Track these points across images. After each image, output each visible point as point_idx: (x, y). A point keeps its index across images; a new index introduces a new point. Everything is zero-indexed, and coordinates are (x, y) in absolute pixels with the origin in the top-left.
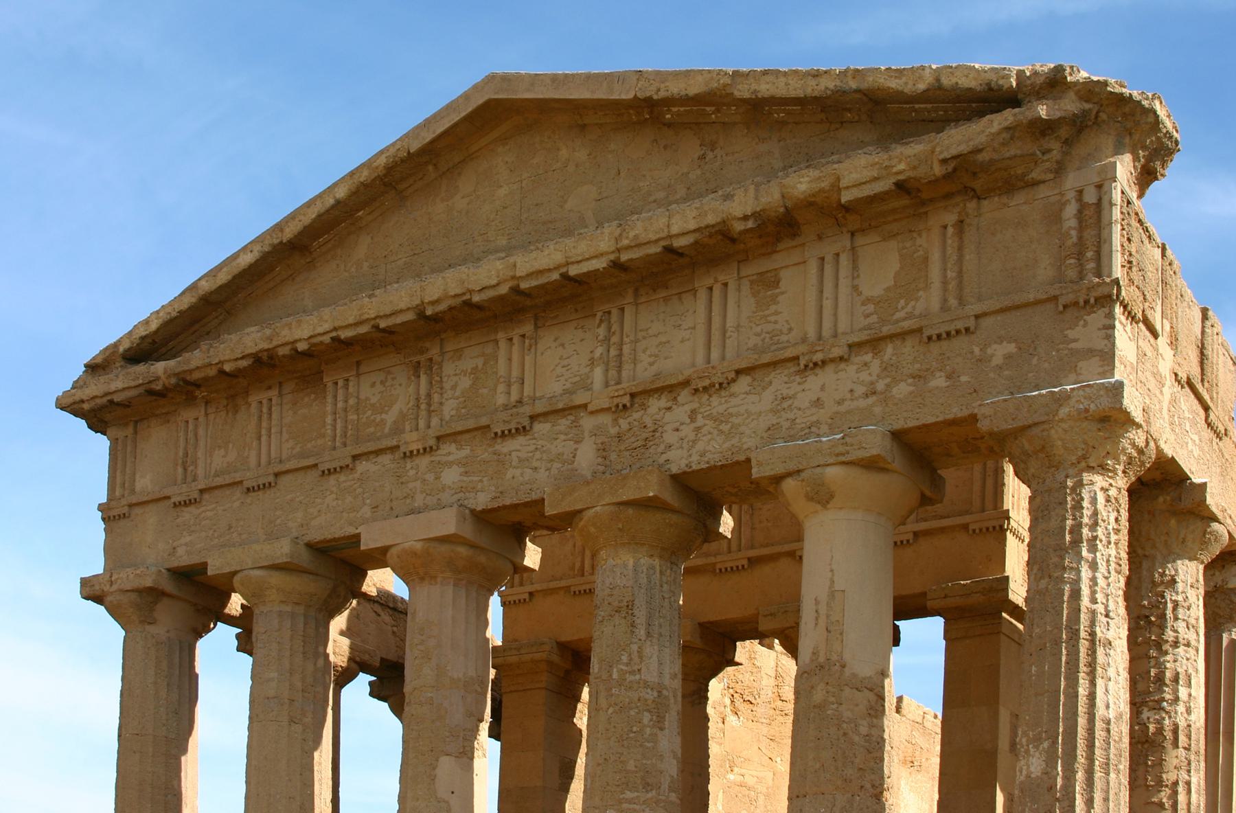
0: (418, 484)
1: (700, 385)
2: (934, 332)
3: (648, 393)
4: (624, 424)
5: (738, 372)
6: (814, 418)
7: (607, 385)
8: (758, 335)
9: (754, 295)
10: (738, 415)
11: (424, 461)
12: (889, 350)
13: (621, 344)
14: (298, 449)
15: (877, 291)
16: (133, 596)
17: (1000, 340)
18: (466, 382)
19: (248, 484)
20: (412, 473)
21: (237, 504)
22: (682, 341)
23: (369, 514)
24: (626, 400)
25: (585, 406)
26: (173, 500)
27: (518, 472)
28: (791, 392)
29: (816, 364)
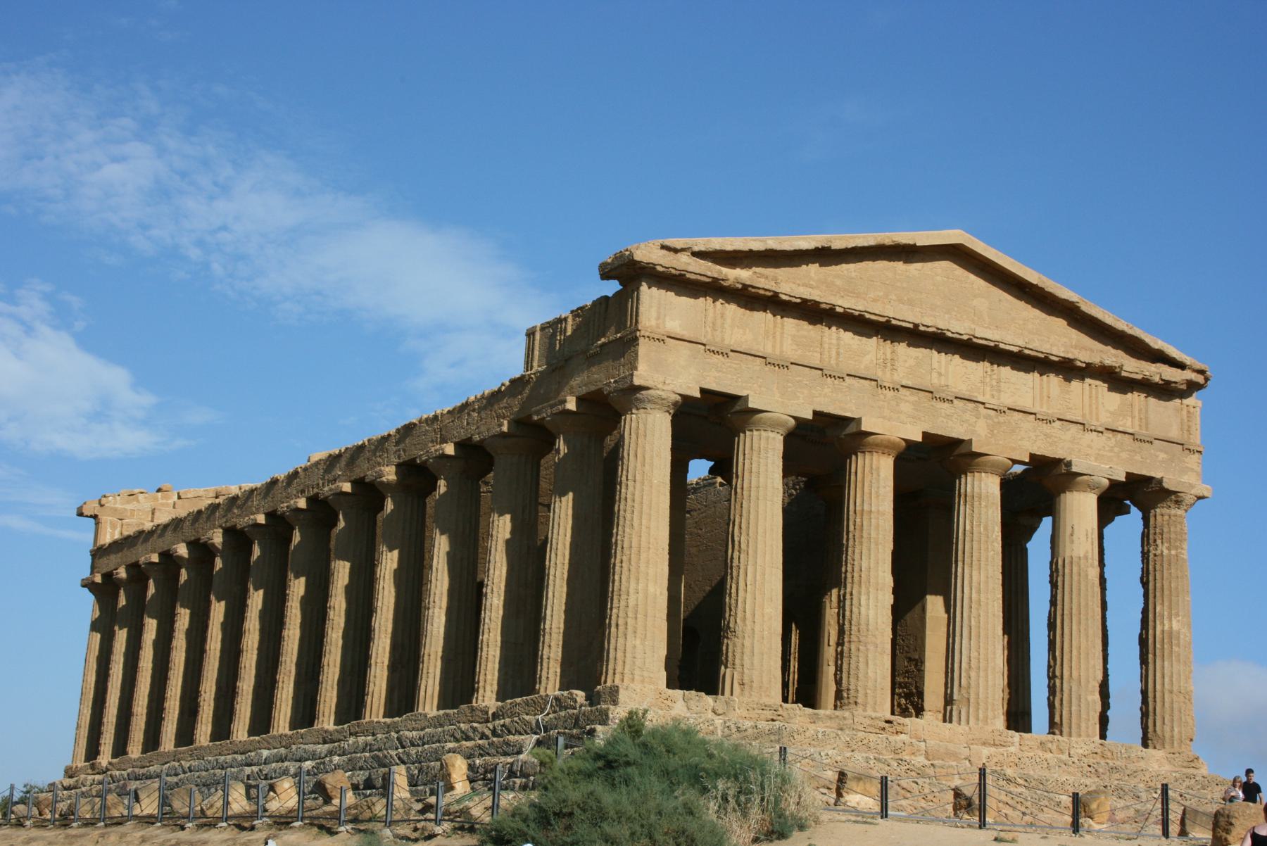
0: (886, 404)
1: (1041, 417)
2: (1139, 438)
3: (1015, 410)
4: (1002, 418)
5: (1059, 419)
6: (1089, 452)
7: (993, 396)
8: (1062, 405)
9: (1060, 386)
10: (1056, 437)
11: (890, 394)
12: (1119, 435)
13: (999, 381)
14: (799, 352)
15: (1112, 409)
16: (679, 398)
17: (1161, 451)
18: (911, 362)
19: (768, 360)
20: (882, 397)
21: (758, 368)
22: (1027, 392)
23: (854, 409)
24: (1006, 409)
25: (983, 403)
26: (708, 347)
27: (945, 420)
28: (1079, 437)
29: (1091, 430)
